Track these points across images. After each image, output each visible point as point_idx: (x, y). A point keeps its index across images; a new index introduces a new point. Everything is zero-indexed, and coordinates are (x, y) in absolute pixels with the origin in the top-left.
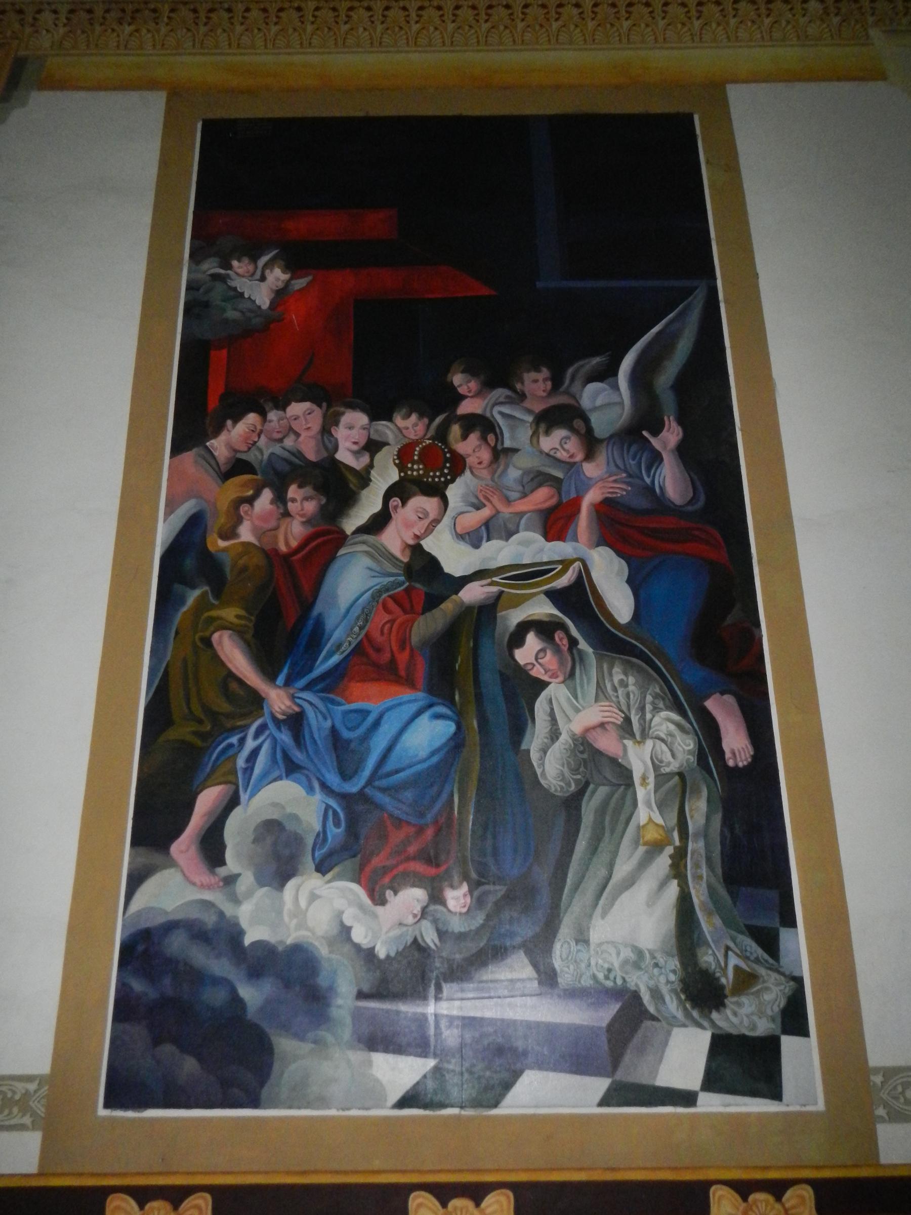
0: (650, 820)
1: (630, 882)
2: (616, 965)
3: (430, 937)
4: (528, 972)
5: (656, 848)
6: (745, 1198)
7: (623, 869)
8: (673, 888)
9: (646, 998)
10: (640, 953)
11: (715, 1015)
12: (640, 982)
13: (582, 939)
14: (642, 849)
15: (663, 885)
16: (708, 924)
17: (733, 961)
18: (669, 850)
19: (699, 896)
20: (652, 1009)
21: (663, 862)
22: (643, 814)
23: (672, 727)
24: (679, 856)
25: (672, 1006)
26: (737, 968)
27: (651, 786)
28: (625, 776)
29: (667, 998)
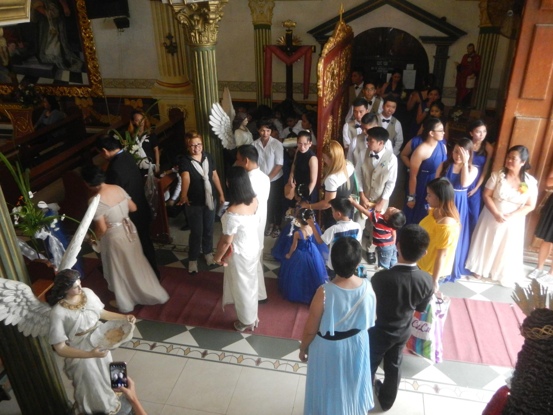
0: (53, 29)
1: (50, 43)
2: (51, 58)
3: (18, 53)
4: (36, 60)
5: (54, 35)
6: (81, 99)
7: (49, 39)
8: (59, 44)
9: (57, 65)
10: (55, 56)
11: (70, 69)
12: (55, 62)
13: (44, 54)
14: (52, 35)
15: (57, 42)
16: (66, 51)
17: (72, 58)
18: (57, 35)
19: (64, 45)
20: (58, 67)
21: (56, 39)
22: (51, 27)
23: (53, 6)
24: (59, 37)
25: (62, 67)
26: (73, 60)
27: (51, 21)
28: (45, 18)
29: (61, 65)
